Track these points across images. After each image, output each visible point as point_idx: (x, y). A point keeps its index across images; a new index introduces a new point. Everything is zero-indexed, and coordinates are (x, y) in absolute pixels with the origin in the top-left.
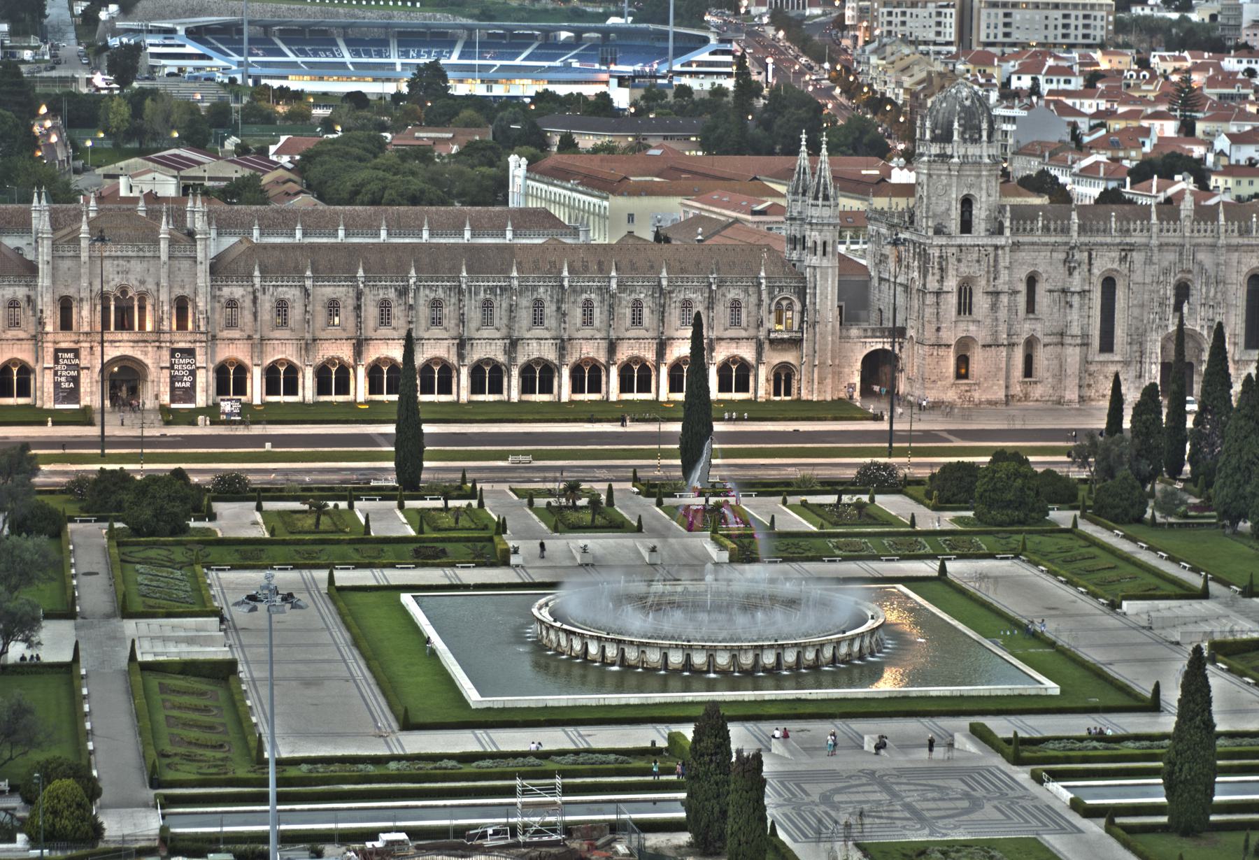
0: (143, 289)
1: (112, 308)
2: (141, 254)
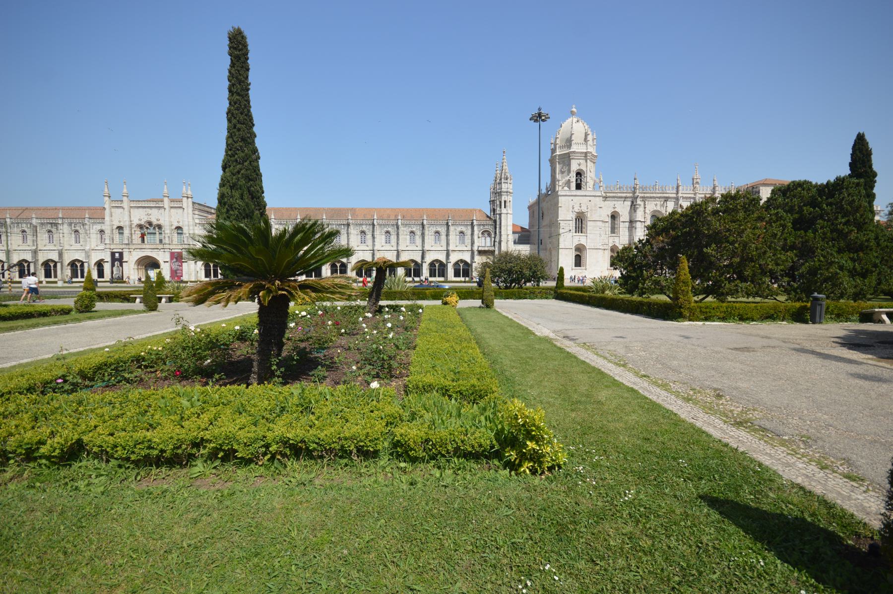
0: (158, 223)
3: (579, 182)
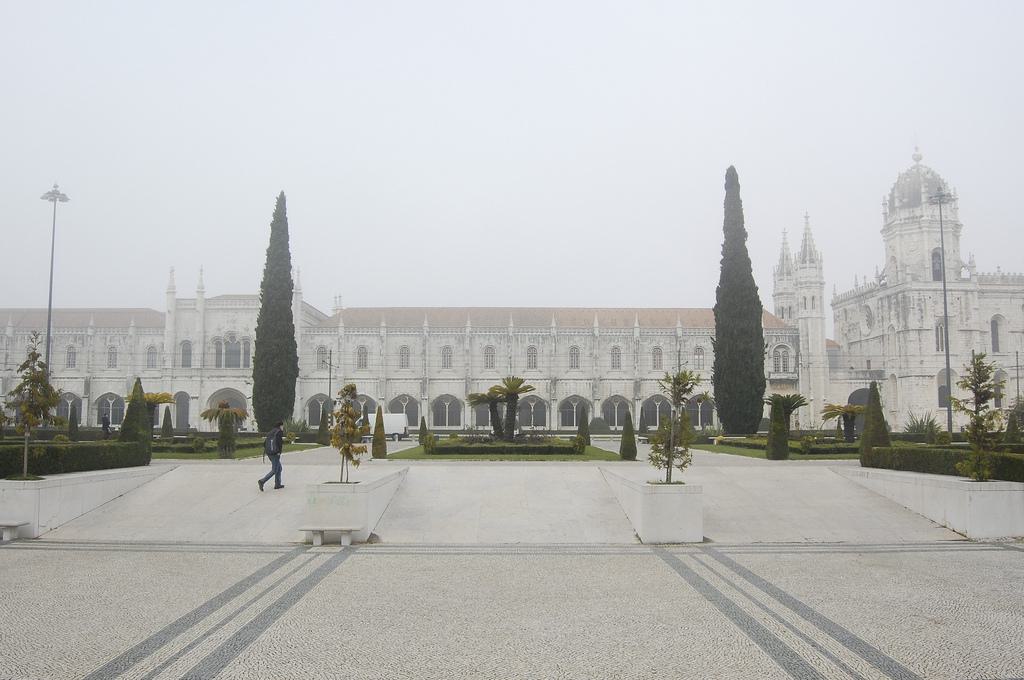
1: (224, 351)
2: (246, 307)
3: (937, 266)
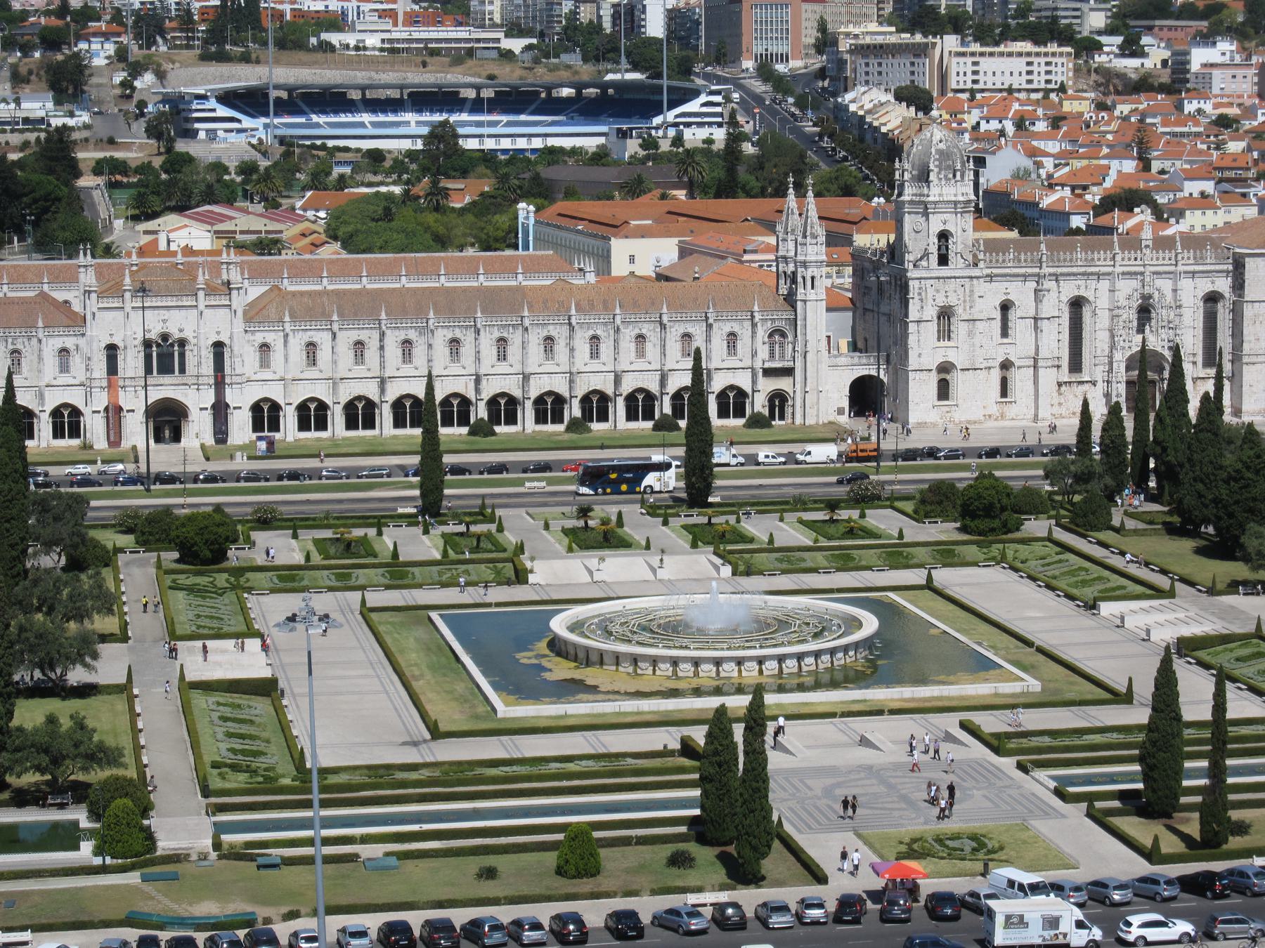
0: (182, 335)
1: (154, 354)
2: (180, 303)
